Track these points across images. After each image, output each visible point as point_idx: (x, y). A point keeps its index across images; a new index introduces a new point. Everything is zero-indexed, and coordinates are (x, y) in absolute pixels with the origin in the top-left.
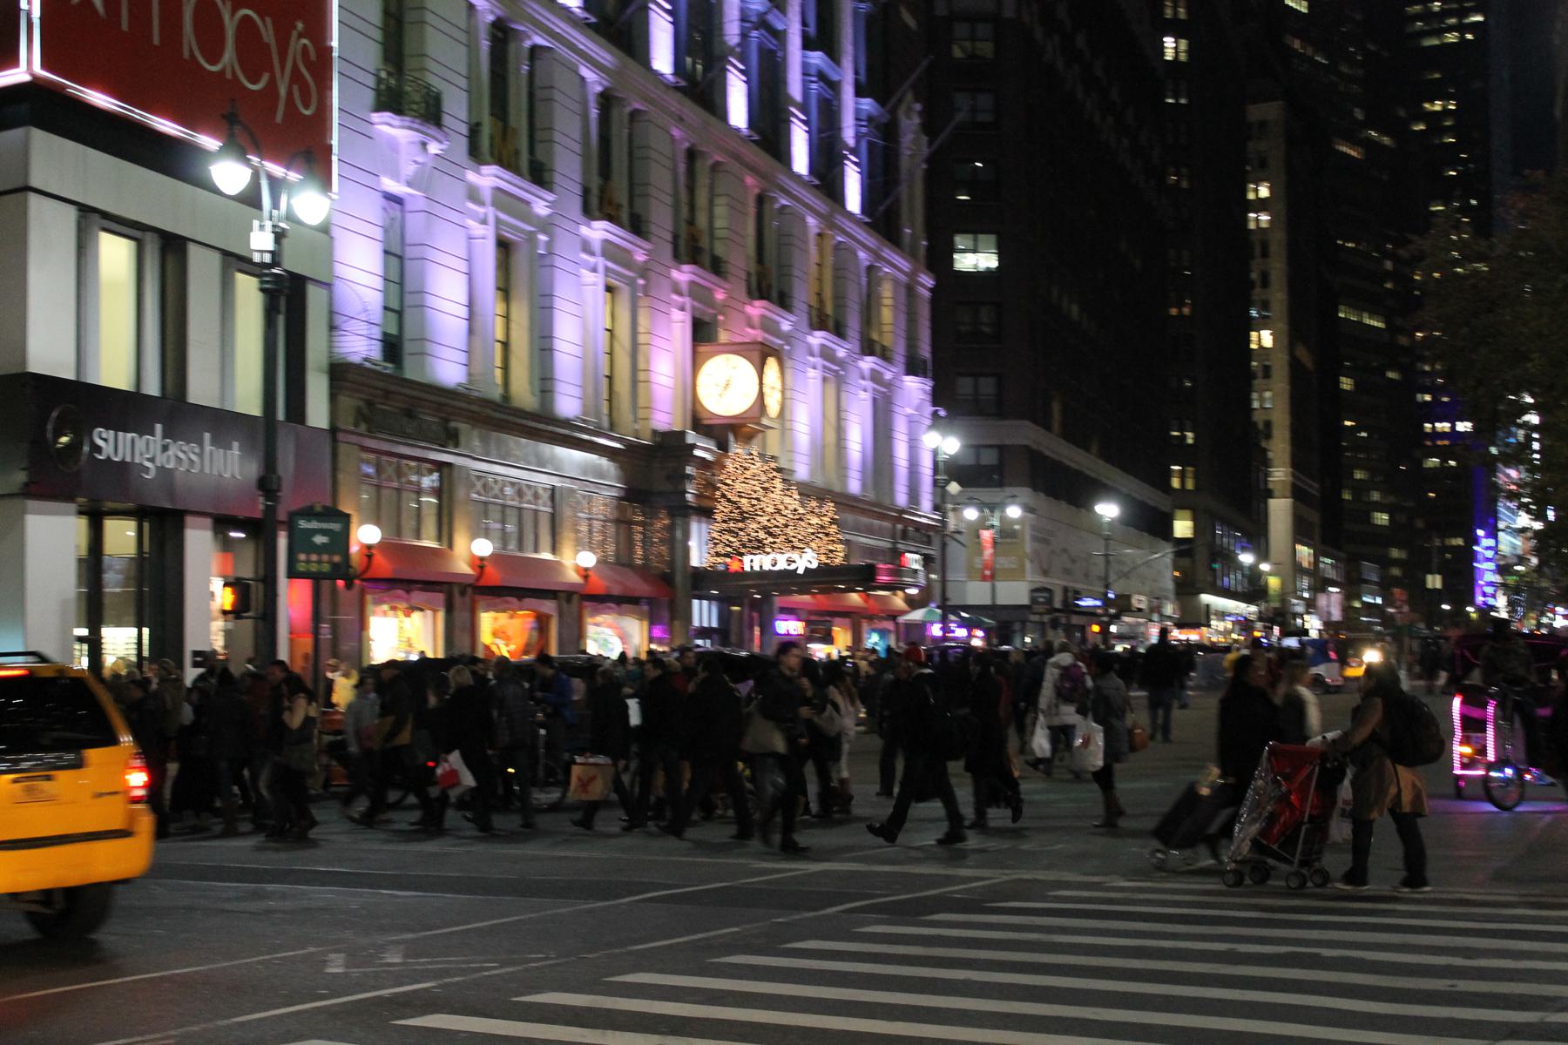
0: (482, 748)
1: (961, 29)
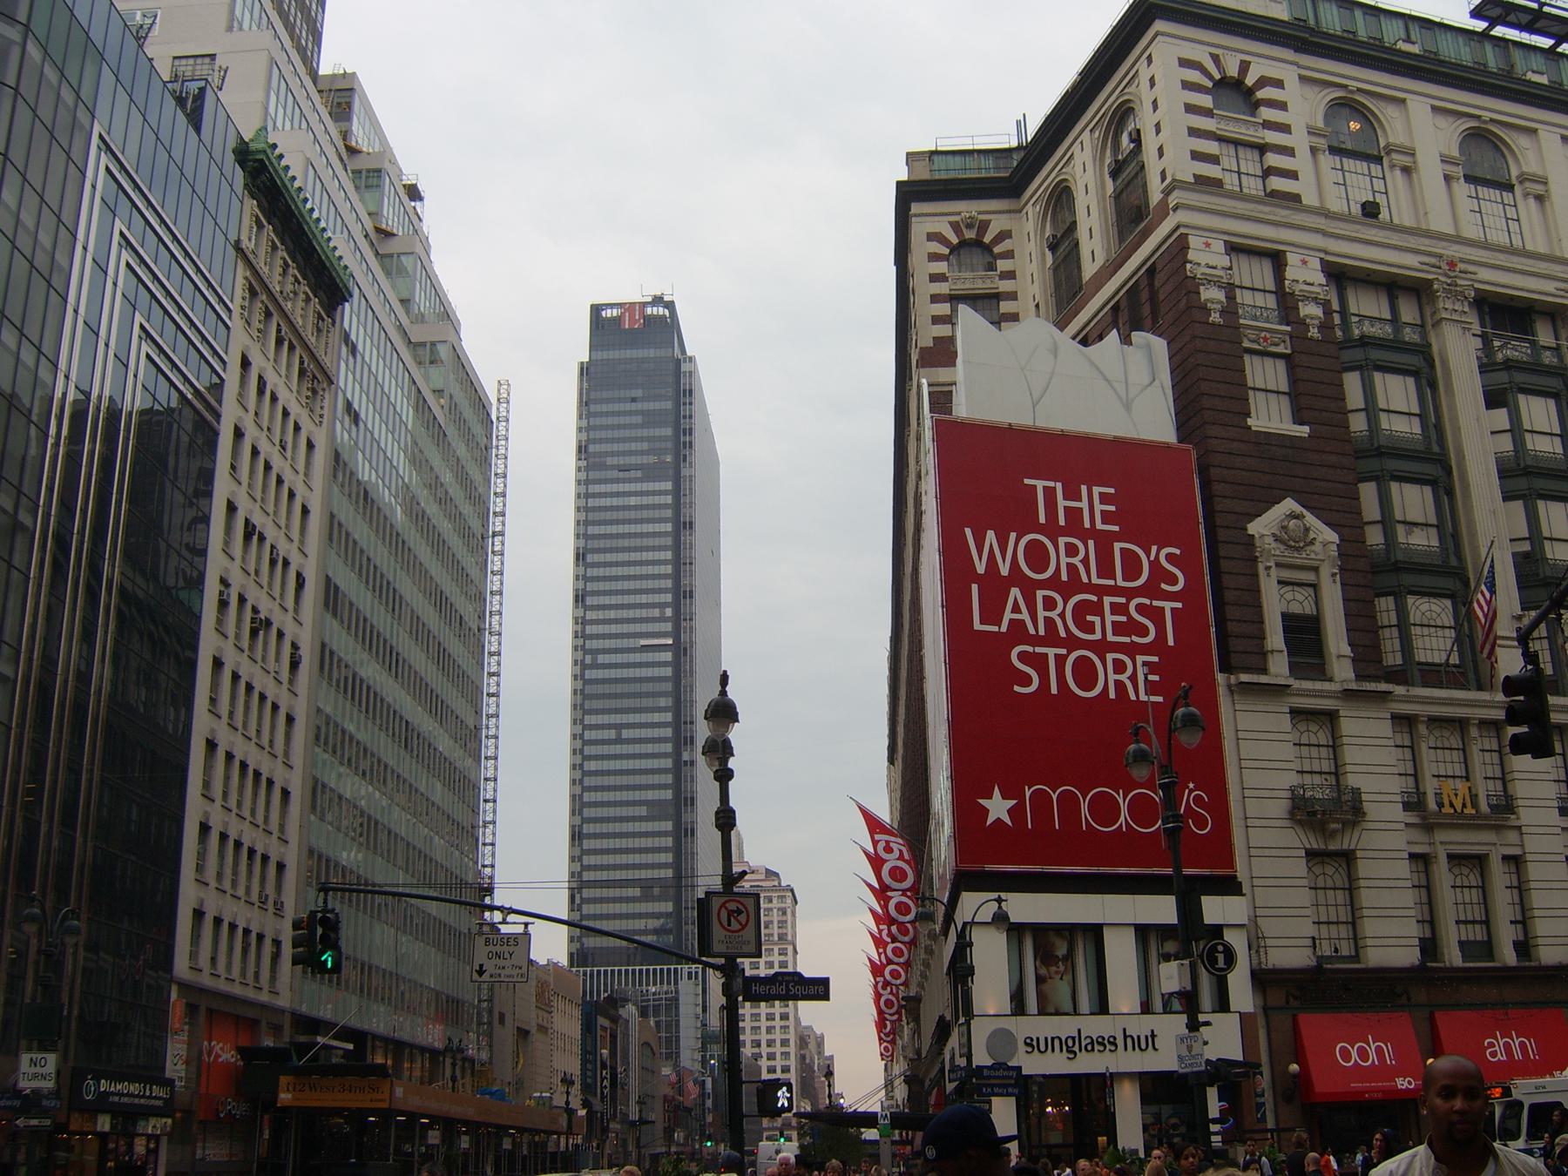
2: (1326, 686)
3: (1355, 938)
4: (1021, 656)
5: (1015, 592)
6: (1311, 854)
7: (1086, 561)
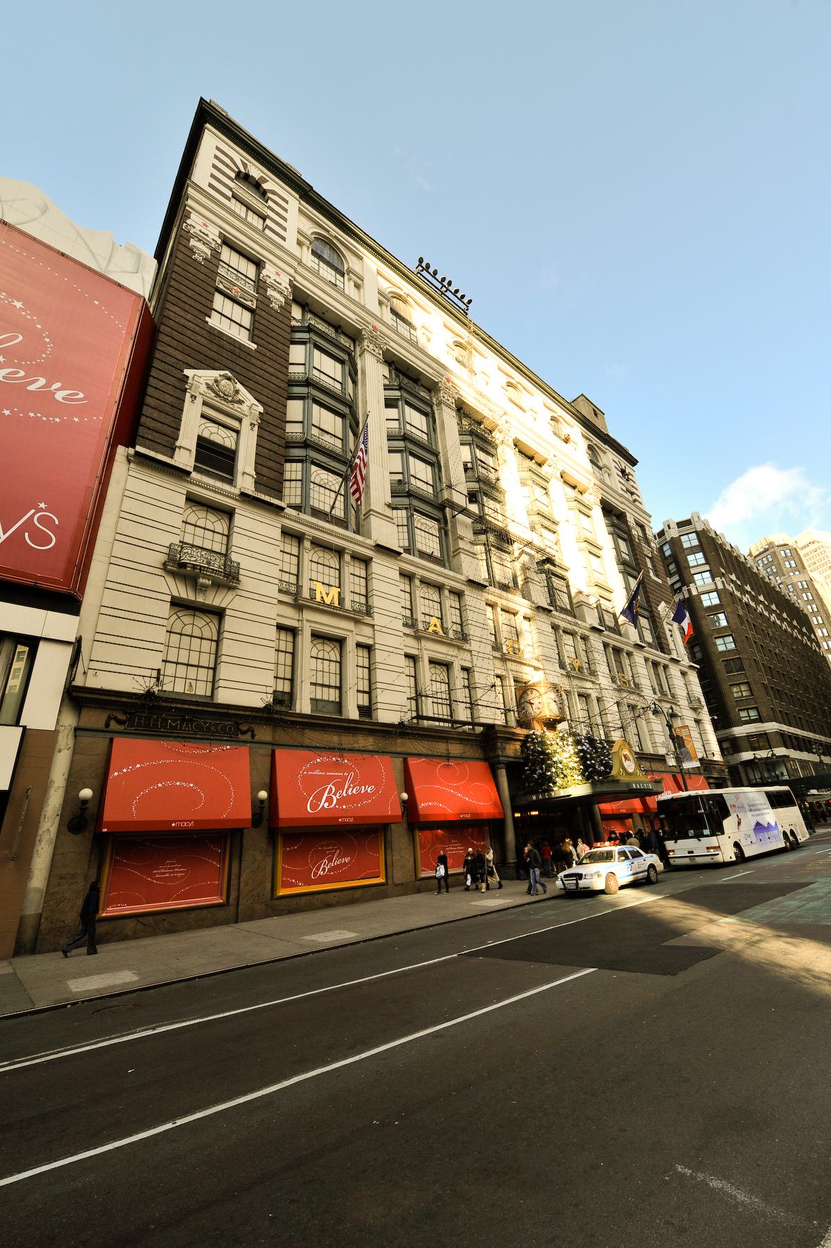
2: (226, 487)
3: (213, 682)
6: (177, 603)
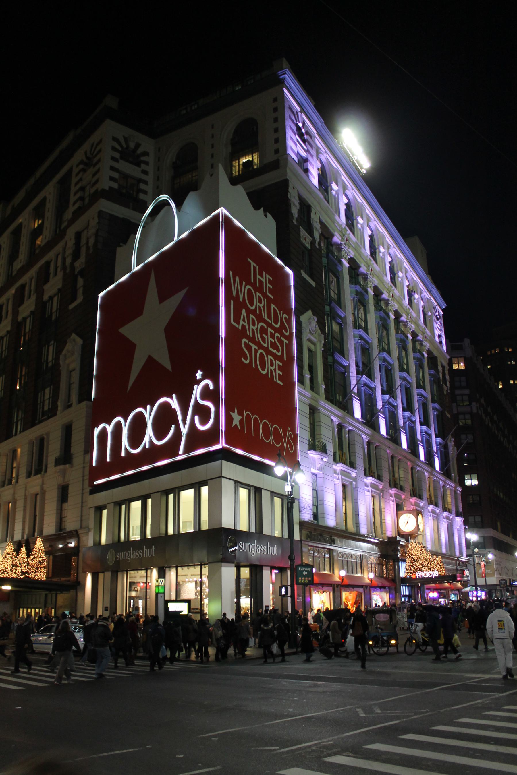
0: (350, 634)
1: (461, 417)
4: (245, 343)
5: (244, 311)
7: (264, 307)
